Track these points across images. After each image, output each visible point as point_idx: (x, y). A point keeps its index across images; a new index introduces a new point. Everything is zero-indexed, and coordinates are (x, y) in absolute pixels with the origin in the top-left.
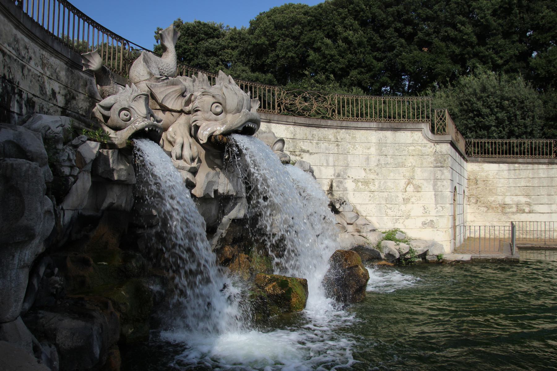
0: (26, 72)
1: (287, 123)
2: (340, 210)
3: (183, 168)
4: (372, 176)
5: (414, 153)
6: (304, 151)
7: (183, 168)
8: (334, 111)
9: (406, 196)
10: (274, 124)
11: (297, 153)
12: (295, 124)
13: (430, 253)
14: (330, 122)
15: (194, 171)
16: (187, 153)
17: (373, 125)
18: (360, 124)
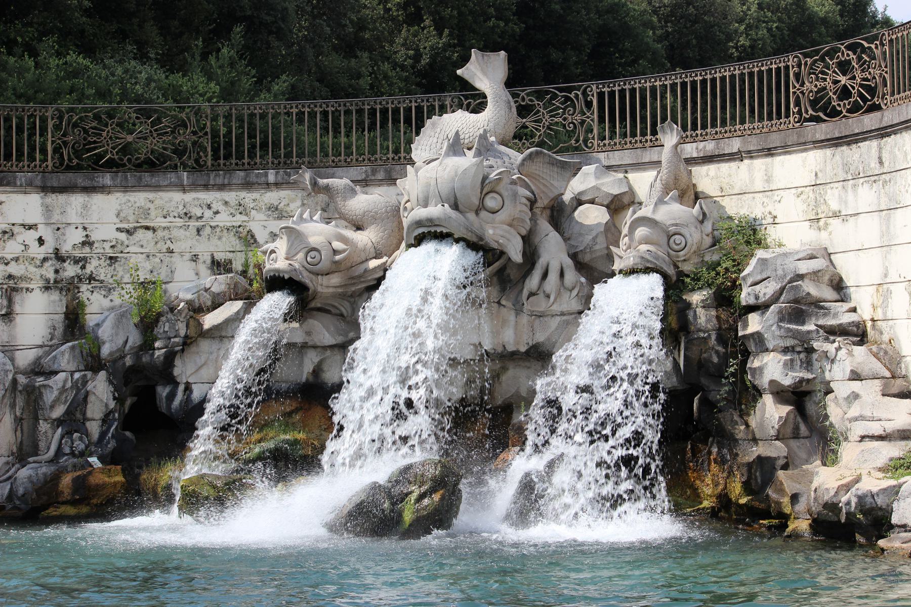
0: (208, 230)
6: (836, 215)
10: (782, 158)
11: (822, 223)
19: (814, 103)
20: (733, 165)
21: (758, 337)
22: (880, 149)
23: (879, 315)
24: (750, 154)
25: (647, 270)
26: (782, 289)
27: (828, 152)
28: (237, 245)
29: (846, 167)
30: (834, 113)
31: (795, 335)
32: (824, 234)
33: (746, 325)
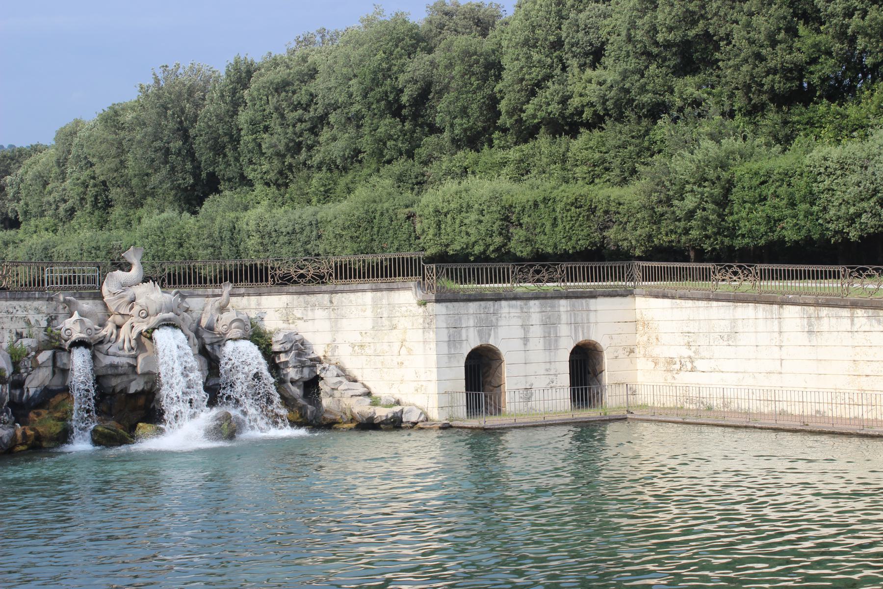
1: (280, 293)
2: (322, 375)
3: (124, 356)
4: (369, 340)
5: (406, 314)
6: (299, 319)
7: (124, 356)
8: (331, 275)
9: (400, 359)
12: (288, 293)
13: (404, 420)
14: (324, 288)
15: (136, 357)
16: (126, 345)
17: (367, 286)
18: (354, 287)
19: (282, 279)
20: (239, 298)
21: (286, 363)
22: (331, 298)
23: (329, 354)
24: (249, 295)
25: (244, 339)
26: (292, 347)
27: (295, 297)
28: (24, 325)
29: (307, 303)
30: (295, 282)
31: (300, 361)
32: (292, 326)
33: (279, 358)
